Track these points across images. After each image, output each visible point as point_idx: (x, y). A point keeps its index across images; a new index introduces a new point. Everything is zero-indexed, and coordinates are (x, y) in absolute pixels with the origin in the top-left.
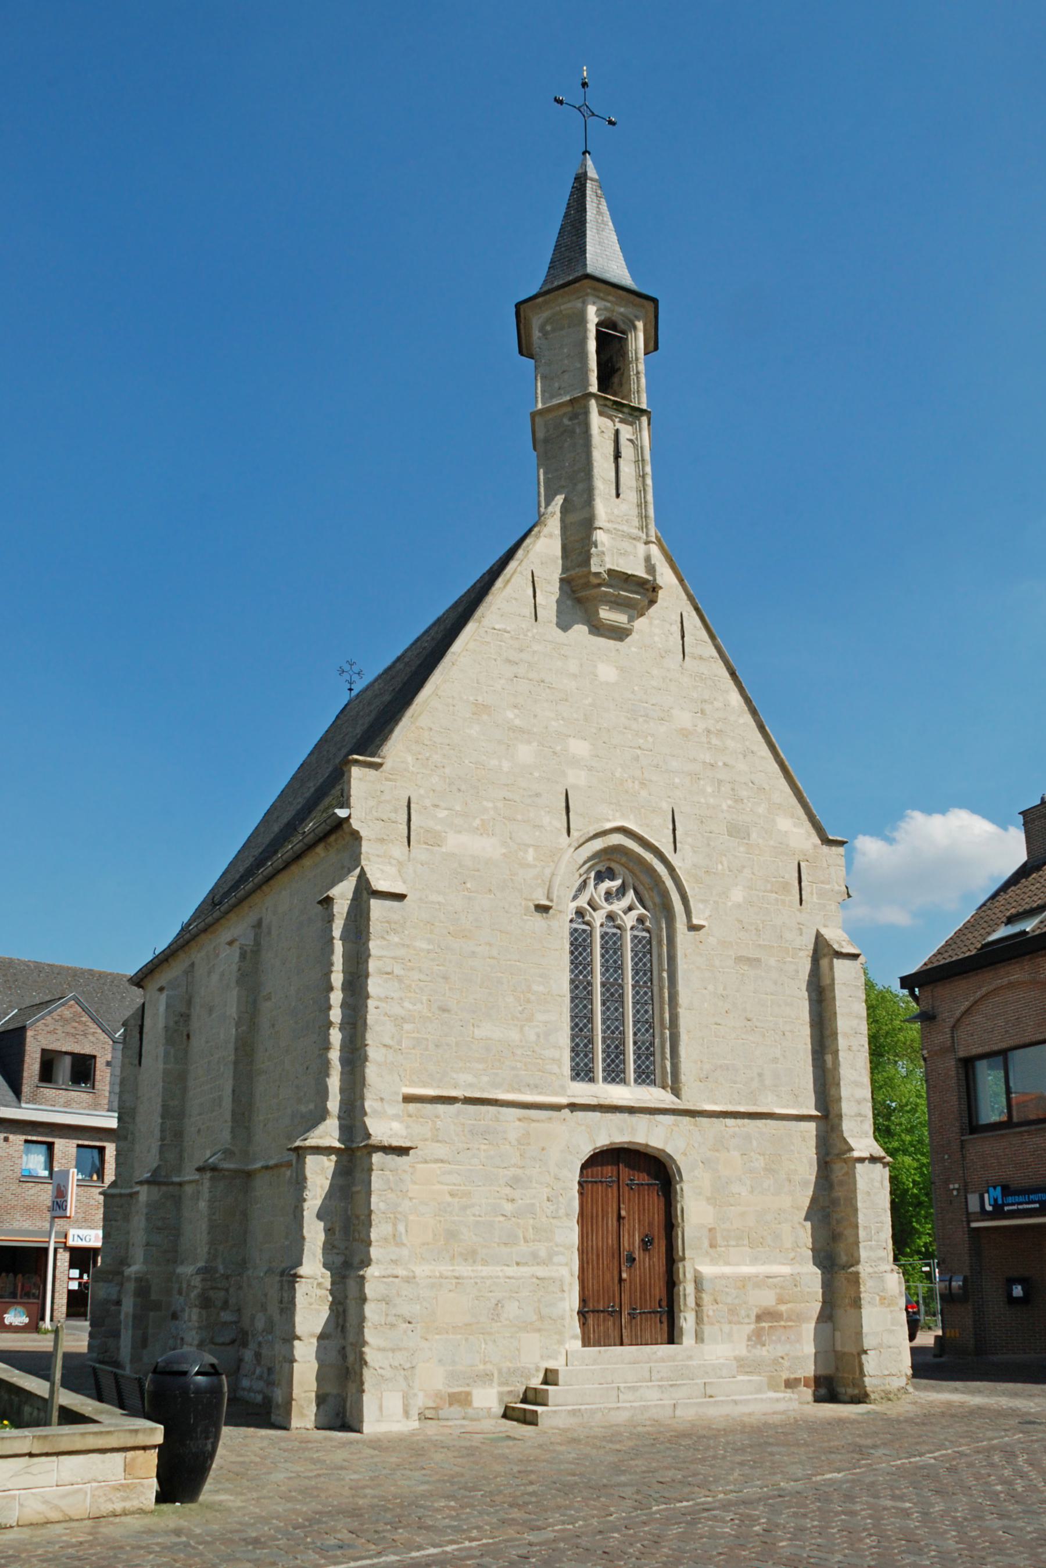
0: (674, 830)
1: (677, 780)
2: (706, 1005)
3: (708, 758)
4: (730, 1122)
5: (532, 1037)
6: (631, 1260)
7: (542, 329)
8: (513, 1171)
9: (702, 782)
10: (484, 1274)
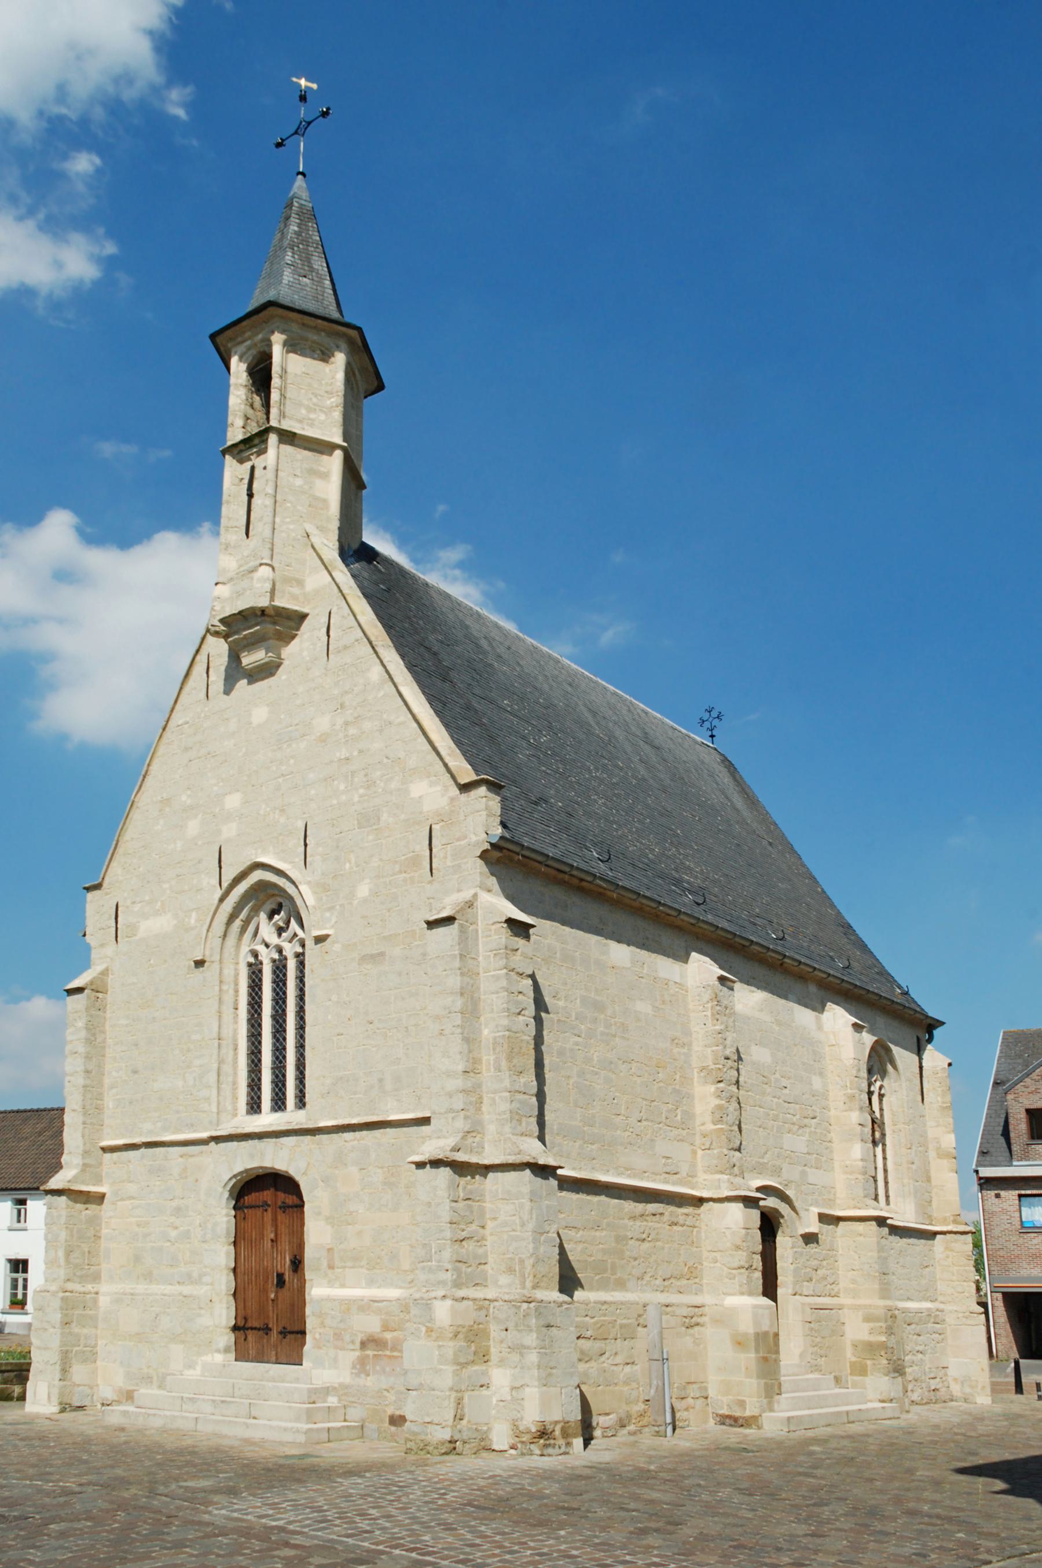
2: (329, 1017)
3: (344, 753)
4: (348, 1136)
8: (176, 1203)
9: (336, 782)
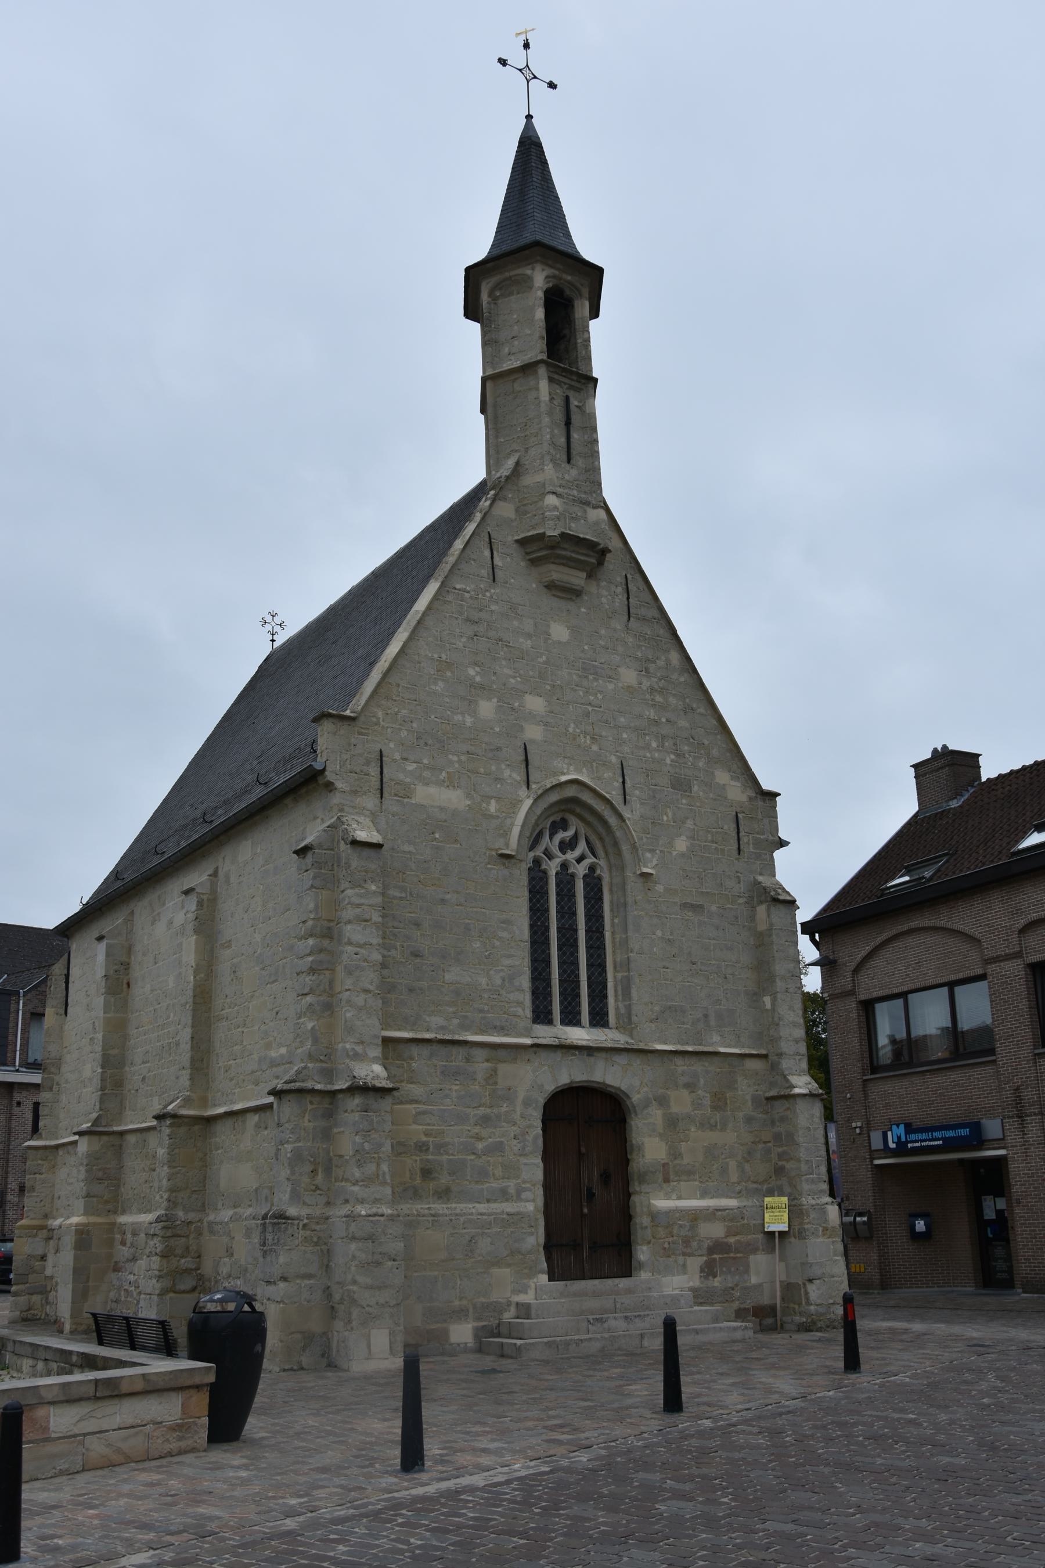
0: (624, 782)
1: (625, 736)
3: (652, 714)
5: (499, 982)
6: (591, 1195)
7: (490, 295)
8: (482, 1111)
10: (458, 1211)
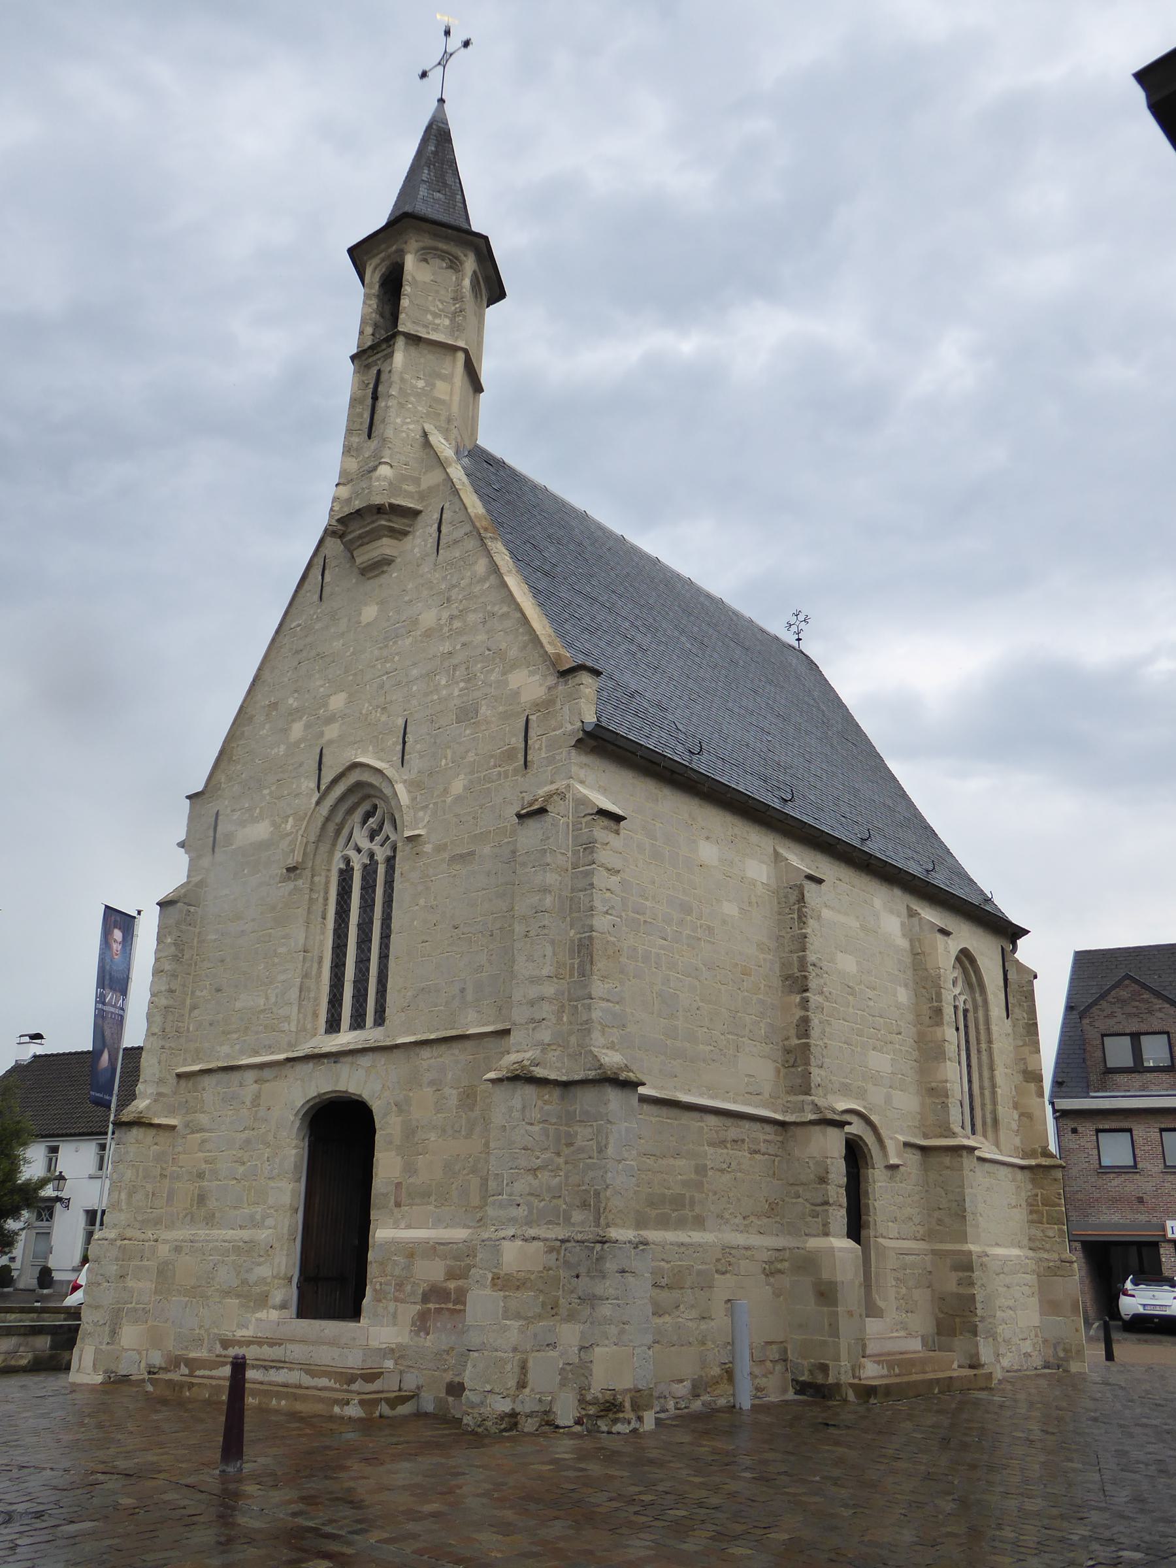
3: (446, 647)
